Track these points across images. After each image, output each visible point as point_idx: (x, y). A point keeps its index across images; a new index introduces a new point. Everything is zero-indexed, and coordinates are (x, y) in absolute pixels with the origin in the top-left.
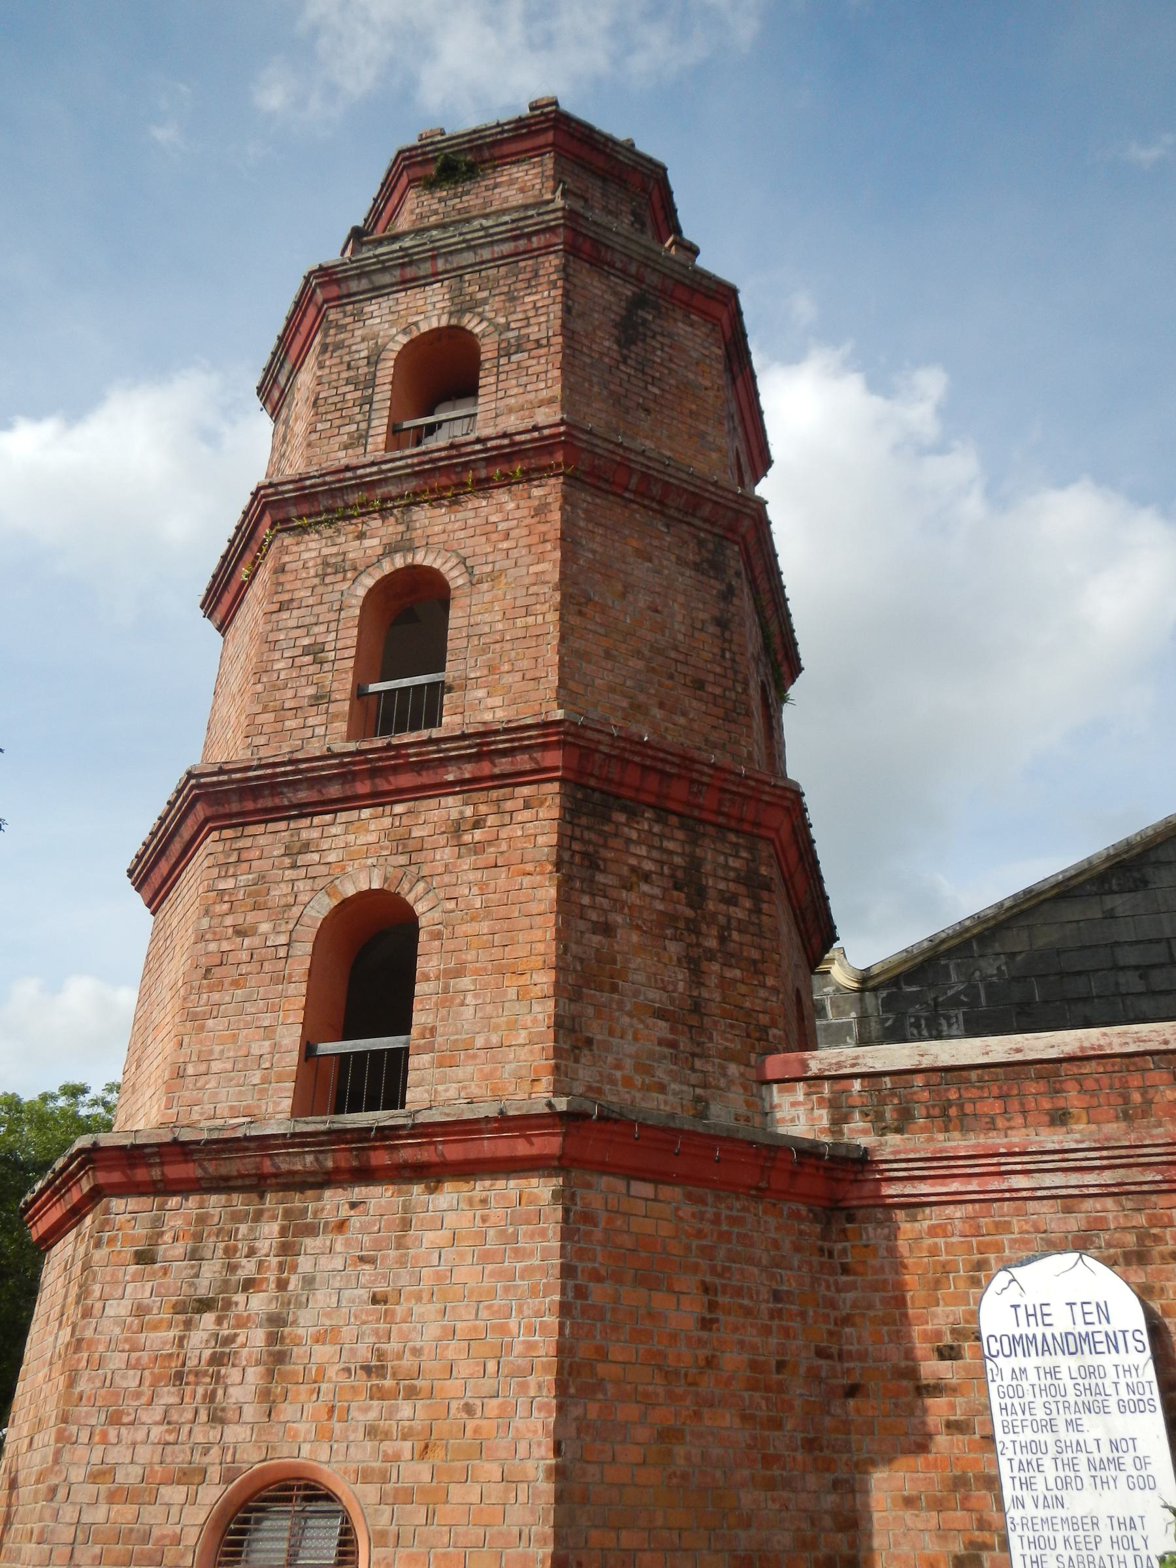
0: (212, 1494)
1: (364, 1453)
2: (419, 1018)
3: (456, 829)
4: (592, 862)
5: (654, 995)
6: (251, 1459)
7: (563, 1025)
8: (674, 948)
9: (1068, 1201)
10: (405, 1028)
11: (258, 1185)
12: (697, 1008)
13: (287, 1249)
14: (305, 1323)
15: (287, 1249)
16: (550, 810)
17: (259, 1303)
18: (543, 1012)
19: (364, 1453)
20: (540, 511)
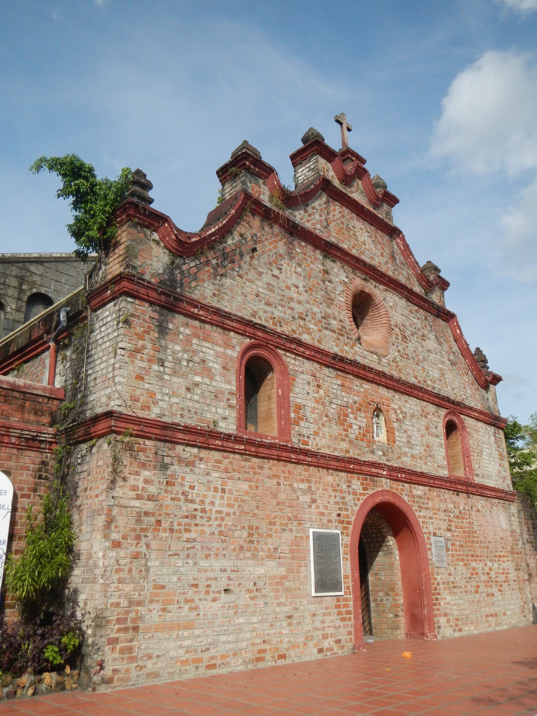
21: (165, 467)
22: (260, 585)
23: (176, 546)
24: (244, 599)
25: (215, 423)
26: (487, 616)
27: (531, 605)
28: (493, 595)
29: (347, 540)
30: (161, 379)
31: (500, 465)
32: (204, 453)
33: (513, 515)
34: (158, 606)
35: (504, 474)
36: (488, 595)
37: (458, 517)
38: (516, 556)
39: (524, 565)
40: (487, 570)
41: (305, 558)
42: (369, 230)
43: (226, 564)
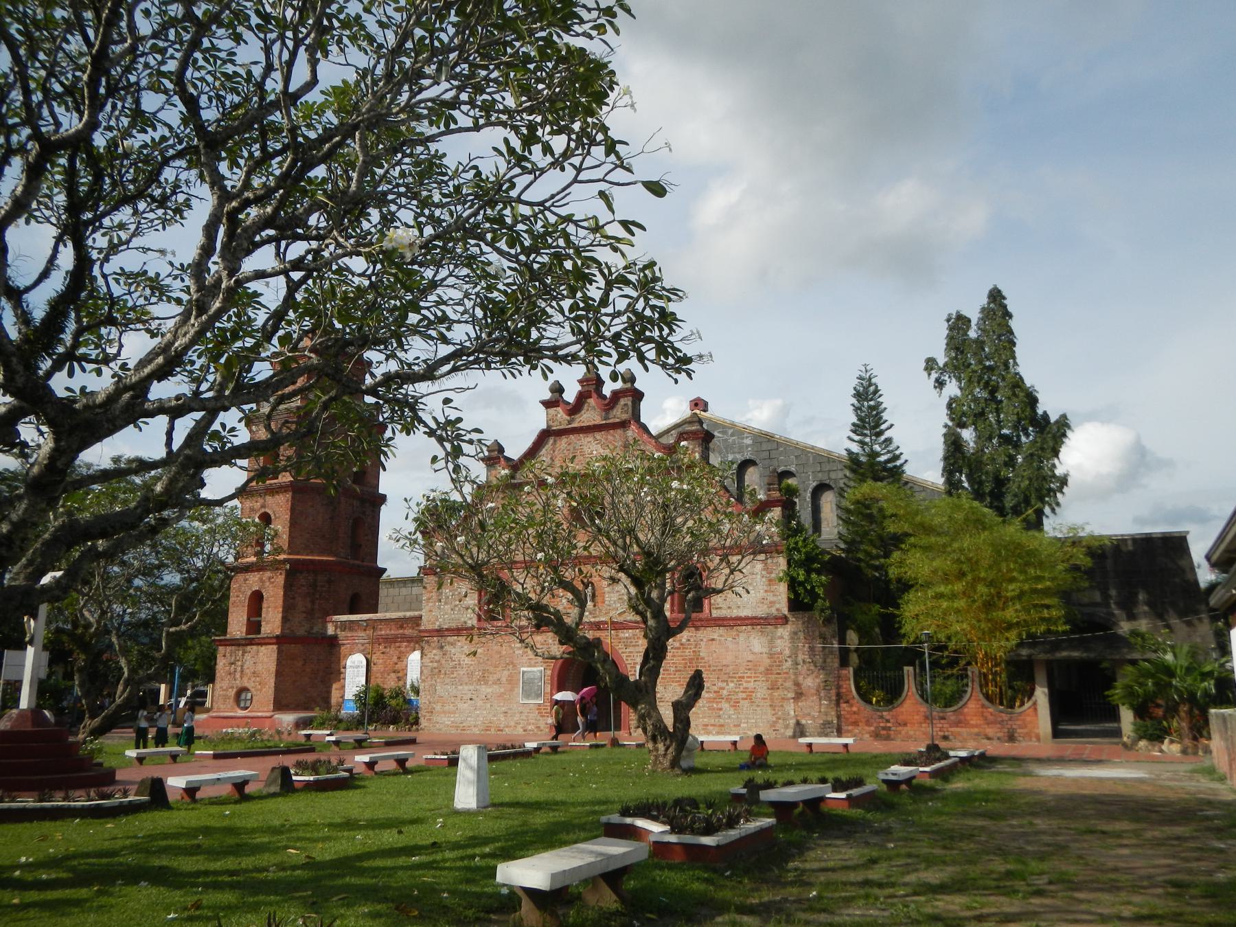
0: (235, 690)
1: (253, 684)
2: (263, 615)
3: (270, 578)
4: (291, 586)
5: (304, 609)
6: (240, 685)
7: (283, 618)
8: (308, 599)
9: (363, 645)
10: (261, 616)
11: (239, 645)
12: (313, 610)
13: (243, 655)
14: (245, 667)
15: (243, 655)
16: (283, 576)
17: (240, 663)
18: (280, 615)
19: (253, 684)
20: (287, 501)
21: (442, 647)
22: (489, 697)
23: (447, 680)
24: (480, 703)
25: (465, 623)
26: (707, 725)
27: (792, 722)
28: (721, 709)
29: (549, 672)
30: (439, 608)
31: (766, 591)
32: (460, 638)
33: (782, 637)
34: (440, 704)
35: (775, 599)
36: (711, 708)
37: (679, 648)
38: (773, 677)
39: (789, 684)
40: (715, 688)
41: (518, 684)
42: (598, 437)
43: (472, 687)
